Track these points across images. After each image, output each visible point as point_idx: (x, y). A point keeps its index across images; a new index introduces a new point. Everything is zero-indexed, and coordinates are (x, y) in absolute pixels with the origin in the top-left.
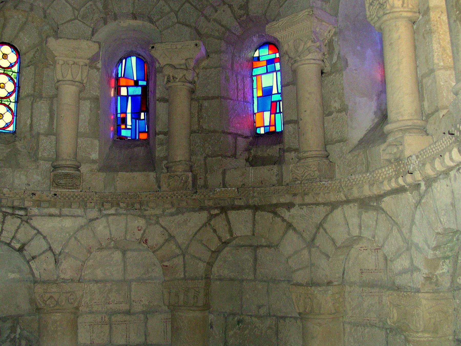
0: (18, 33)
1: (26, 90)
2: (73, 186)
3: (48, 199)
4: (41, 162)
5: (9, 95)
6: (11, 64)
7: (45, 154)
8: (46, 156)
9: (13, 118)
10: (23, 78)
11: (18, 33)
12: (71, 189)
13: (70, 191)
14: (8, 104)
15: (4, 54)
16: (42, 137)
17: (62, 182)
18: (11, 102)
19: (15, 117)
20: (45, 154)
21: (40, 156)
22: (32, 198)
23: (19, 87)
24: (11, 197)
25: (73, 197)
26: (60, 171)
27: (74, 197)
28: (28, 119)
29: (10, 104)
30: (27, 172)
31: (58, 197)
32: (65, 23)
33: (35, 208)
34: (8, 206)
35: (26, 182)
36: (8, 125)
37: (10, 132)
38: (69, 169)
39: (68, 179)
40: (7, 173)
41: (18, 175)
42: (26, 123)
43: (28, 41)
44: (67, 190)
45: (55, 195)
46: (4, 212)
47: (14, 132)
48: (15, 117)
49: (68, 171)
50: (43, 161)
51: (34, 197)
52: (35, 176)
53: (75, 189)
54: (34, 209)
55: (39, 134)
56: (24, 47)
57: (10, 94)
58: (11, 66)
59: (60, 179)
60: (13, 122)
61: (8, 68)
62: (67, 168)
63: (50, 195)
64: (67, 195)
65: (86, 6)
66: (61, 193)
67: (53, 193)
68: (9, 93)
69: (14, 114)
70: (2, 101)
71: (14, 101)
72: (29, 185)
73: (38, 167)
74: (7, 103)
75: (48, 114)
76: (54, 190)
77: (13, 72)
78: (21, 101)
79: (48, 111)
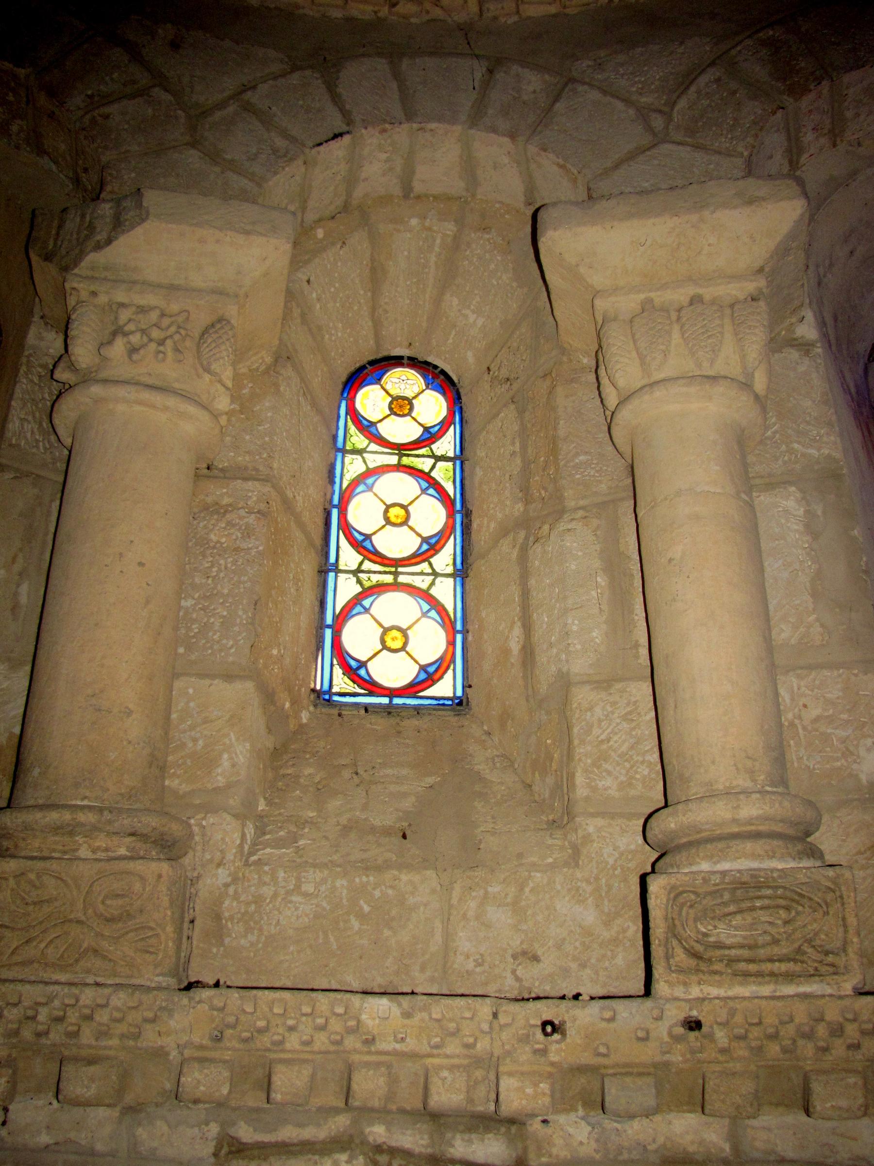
0: (438, 301)
1: (497, 508)
2: (796, 956)
3: (649, 1053)
4: (591, 826)
5: (425, 547)
6: (426, 429)
7: (608, 782)
8: (613, 793)
9: (451, 643)
10: (479, 472)
11: (438, 301)
12: (790, 977)
13: (789, 990)
14: (424, 586)
15: (395, 399)
16: (582, 696)
17: (723, 932)
18: (435, 574)
19: (459, 637)
20: (608, 782)
21: (581, 791)
22: (544, 1052)
23: (467, 514)
24: (414, 1056)
25: (809, 1036)
26: (705, 866)
27: (821, 1030)
28: (512, 628)
29: (433, 583)
30: (522, 889)
31: (711, 1037)
32: (616, 166)
33: (573, 1116)
34: (402, 1111)
35: (517, 943)
36: (430, 675)
37: (441, 704)
38: (759, 846)
39: (764, 916)
40: (411, 900)
41: (473, 904)
42: (507, 652)
43: (480, 322)
44: (766, 990)
45: (694, 1025)
46: (379, 1149)
47: (460, 704)
48: (459, 637)
49: (755, 865)
50: (600, 822)
51: (558, 1050)
52: (563, 906)
53: (816, 974)
54: (562, 1119)
55: (565, 683)
56: (470, 354)
57: (432, 546)
58: (429, 437)
59: (705, 915)
60: (453, 660)
61: (417, 444)
62: (749, 845)
63: (662, 1030)
64: (770, 1020)
65: (693, 89)
66: (732, 1013)
67: (675, 1014)
68: (425, 540)
69: (453, 624)
70: (396, 574)
71: (450, 570)
72: (536, 959)
73: (575, 856)
74: (422, 583)
75: (602, 580)
76: (679, 992)
77: (439, 459)
78: (479, 567)
79: (597, 564)
